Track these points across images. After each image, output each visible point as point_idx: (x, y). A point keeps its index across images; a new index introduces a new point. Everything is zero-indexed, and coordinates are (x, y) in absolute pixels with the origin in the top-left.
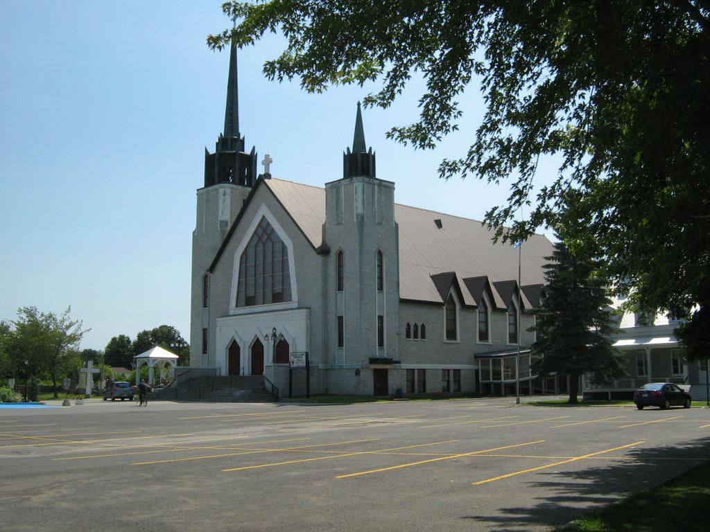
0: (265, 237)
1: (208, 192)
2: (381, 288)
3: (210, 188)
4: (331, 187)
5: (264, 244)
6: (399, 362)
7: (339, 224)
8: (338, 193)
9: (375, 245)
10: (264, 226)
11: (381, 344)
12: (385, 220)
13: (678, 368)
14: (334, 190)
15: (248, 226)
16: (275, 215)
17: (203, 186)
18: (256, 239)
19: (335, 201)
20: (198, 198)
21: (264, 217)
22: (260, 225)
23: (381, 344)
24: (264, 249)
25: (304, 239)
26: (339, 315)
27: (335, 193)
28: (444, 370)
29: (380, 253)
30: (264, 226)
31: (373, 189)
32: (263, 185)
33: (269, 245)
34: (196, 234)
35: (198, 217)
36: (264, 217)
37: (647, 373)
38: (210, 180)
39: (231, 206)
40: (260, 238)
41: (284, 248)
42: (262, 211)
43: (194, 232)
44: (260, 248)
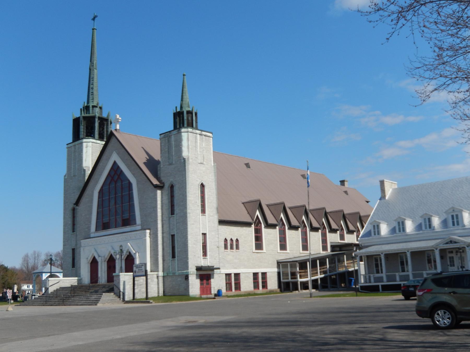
0: (116, 177)
1: (75, 146)
2: (203, 211)
3: (76, 143)
4: (164, 137)
5: (116, 182)
6: (219, 269)
7: (171, 164)
8: (169, 141)
9: (198, 179)
10: (115, 167)
11: (205, 254)
12: (205, 160)
13: (379, 269)
14: (167, 138)
15: (97, 182)
16: (122, 159)
17: (71, 141)
18: (110, 178)
19: (167, 147)
20: (68, 151)
21: (115, 163)
22: (112, 168)
23: (205, 254)
24: (115, 186)
25: (144, 176)
26: (172, 234)
27: (167, 141)
28: (226, 274)
29: (202, 186)
30: (115, 167)
31: (196, 138)
32: (114, 138)
33: (119, 184)
34: (66, 177)
35: (65, 187)
36: (115, 163)
37: (382, 273)
38: (77, 137)
39: (92, 155)
40: (113, 178)
41: (130, 184)
42: (115, 157)
43: (65, 176)
44: (113, 185)
